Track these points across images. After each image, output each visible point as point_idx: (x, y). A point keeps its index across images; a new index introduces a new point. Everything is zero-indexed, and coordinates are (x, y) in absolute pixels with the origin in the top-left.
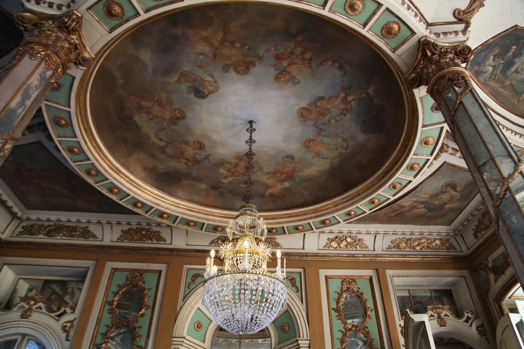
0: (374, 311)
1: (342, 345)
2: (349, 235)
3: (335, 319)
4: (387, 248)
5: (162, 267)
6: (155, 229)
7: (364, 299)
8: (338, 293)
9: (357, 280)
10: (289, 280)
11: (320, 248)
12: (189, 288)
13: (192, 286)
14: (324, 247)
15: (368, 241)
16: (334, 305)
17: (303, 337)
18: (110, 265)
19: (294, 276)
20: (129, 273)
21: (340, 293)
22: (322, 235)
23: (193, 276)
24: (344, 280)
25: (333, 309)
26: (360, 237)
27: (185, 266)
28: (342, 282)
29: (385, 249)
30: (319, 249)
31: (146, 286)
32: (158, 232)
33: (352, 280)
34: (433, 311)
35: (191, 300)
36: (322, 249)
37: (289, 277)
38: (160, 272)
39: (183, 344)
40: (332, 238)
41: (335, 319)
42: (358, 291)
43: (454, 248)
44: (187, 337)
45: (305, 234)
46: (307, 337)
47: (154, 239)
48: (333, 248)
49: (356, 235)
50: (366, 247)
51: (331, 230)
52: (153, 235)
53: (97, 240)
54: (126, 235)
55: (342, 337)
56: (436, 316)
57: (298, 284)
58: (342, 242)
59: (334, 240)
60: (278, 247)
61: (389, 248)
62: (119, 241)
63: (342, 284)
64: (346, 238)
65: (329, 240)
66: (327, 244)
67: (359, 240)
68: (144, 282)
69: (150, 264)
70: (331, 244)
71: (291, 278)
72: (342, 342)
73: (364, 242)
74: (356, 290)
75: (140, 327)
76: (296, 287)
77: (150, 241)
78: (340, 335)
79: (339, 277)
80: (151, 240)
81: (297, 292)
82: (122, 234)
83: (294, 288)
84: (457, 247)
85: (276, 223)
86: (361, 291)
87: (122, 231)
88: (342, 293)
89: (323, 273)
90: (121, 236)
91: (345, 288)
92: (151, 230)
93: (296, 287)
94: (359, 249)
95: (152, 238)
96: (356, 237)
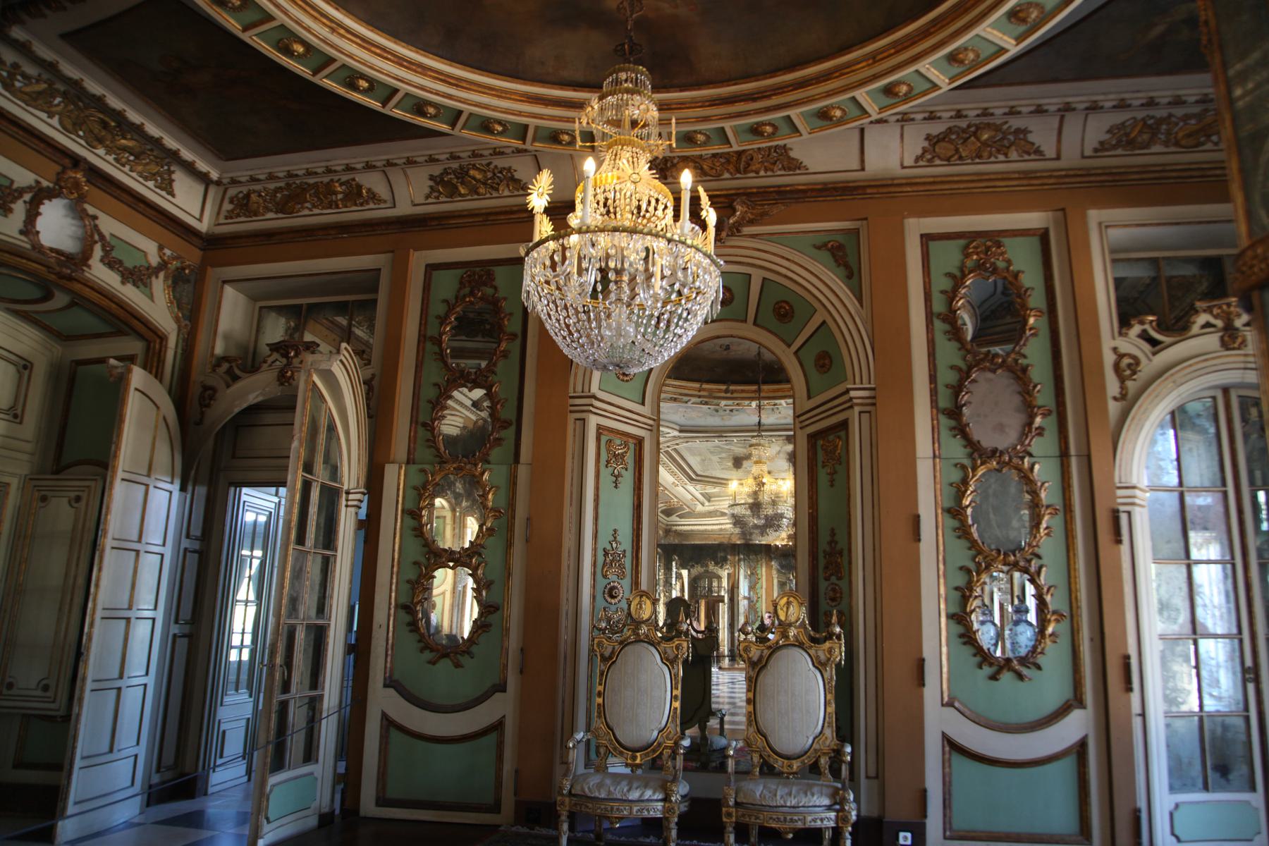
2: (986, 120)
3: (940, 339)
6: (500, 162)
7: (1022, 287)
9: (1006, 241)
10: (829, 250)
11: (906, 164)
14: (917, 160)
15: (1042, 134)
16: (939, 306)
17: (862, 383)
18: (419, 260)
20: (464, 270)
21: (958, 274)
22: (909, 129)
24: (970, 237)
25: (939, 315)
26: (1015, 123)
28: (967, 247)
29: (1088, 152)
30: (903, 167)
32: (509, 169)
33: (995, 238)
34: (1211, 313)
36: (913, 164)
37: (829, 242)
39: (591, 408)
40: (936, 134)
41: (940, 339)
42: (1007, 269)
44: (600, 395)
45: (862, 131)
46: (870, 383)
47: (501, 188)
48: (942, 159)
49: (1006, 118)
50: (1038, 151)
51: (931, 112)
52: (498, 177)
53: (382, 206)
54: (444, 184)
56: (1219, 323)
58: (966, 140)
59: (944, 138)
60: (798, 172)
61: (1102, 147)
62: (430, 200)
63: (967, 256)
64: (975, 134)
65: (930, 140)
66: (925, 151)
67: (1018, 131)
68: (496, 288)
70: (934, 150)
71: (832, 245)
72: (957, 390)
73: (1031, 138)
74: (1001, 264)
76: (847, 266)
77: (495, 194)
80: (497, 190)
81: (850, 276)
82: (431, 183)
83: (842, 268)
85: (768, 110)
87: (432, 178)
88: (964, 276)
89: (916, 227)
90: (431, 187)
91: (969, 263)
92: (492, 166)
95: (498, 184)
96: (1005, 127)
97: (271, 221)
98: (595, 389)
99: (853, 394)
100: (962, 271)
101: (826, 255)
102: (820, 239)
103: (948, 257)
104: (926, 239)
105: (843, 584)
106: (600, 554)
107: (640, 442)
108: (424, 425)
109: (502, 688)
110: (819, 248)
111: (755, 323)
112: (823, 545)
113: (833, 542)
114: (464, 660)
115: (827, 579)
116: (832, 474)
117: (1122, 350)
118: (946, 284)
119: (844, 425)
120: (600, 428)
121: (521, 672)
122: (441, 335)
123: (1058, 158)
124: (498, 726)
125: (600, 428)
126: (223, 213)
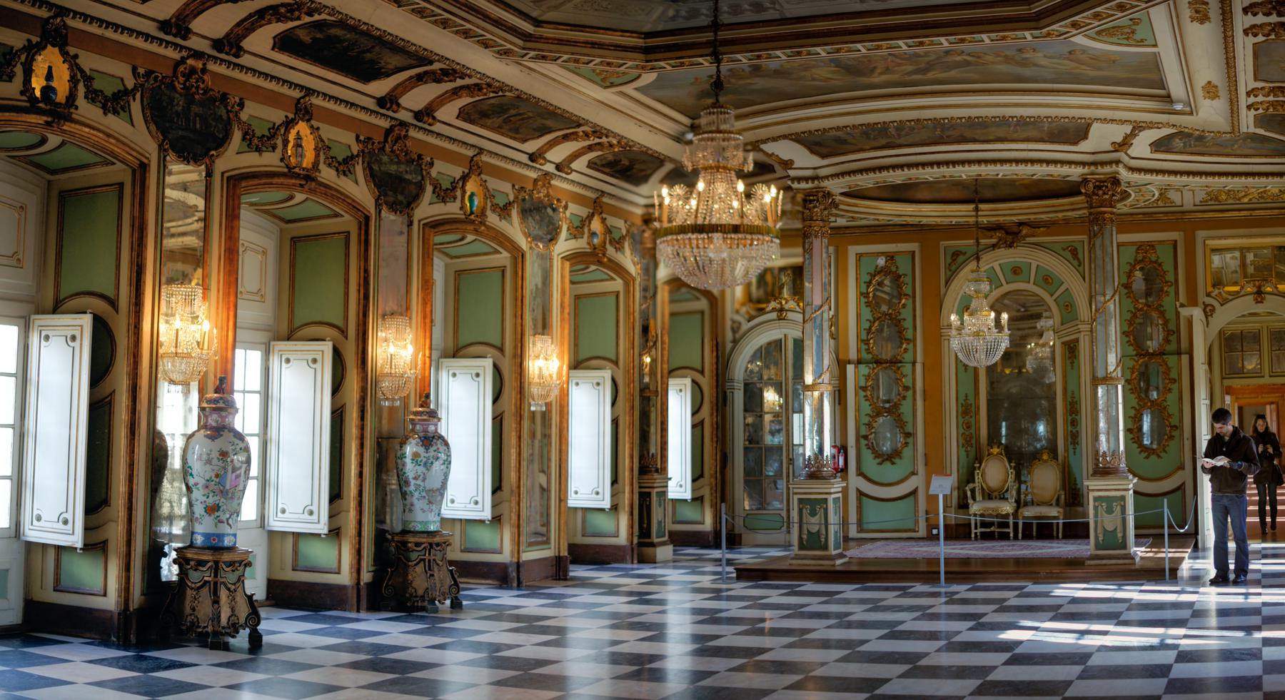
0: (1173, 287)
1: (1129, 328)
4: (1201, 202)
5: (914, 246)
8: (1131, 264)
9: (1157, 247)
12: (950, 270)
13: (953, 268)
16: (1124, 280)
18: (853, 250)
19: (1076, 245)
23: (953, 254)
24: (1140, 246)
27: (941, 243)
28: (1138, 249)
29: (1198, 203)
31: (900, 272)
33: (1152, 245)
35: (954, 285)
55: (1131, 318)
57: (1080, 256)
63: (1137, 253)
68: (897, 267)
69: (899, 245)
74: (1153, 259)
75: (904, 319)
79: (1132, 243)
81: (1079, 266)
86: (1160, 261)
91: (1140, 258)
93: (1078, 259)
94: (1162, 205)
99: (1080, 326)
100: (1135, 260)
101: (1069, 255)
103: (1129, 254)
105: (1078, 418)
106: (960, 405)
108: (862, 341)
109: (913, 473)
110: (1064, 250)
111: (1034, 284)
114: (897, 461)
115: (1071, 415)
117: (1207, 303)
118: (1128, 268)
119: (1077, 340)
121: (926, 465)
122: (868, 293)
123: (1182, 206)
124: (914, 493)
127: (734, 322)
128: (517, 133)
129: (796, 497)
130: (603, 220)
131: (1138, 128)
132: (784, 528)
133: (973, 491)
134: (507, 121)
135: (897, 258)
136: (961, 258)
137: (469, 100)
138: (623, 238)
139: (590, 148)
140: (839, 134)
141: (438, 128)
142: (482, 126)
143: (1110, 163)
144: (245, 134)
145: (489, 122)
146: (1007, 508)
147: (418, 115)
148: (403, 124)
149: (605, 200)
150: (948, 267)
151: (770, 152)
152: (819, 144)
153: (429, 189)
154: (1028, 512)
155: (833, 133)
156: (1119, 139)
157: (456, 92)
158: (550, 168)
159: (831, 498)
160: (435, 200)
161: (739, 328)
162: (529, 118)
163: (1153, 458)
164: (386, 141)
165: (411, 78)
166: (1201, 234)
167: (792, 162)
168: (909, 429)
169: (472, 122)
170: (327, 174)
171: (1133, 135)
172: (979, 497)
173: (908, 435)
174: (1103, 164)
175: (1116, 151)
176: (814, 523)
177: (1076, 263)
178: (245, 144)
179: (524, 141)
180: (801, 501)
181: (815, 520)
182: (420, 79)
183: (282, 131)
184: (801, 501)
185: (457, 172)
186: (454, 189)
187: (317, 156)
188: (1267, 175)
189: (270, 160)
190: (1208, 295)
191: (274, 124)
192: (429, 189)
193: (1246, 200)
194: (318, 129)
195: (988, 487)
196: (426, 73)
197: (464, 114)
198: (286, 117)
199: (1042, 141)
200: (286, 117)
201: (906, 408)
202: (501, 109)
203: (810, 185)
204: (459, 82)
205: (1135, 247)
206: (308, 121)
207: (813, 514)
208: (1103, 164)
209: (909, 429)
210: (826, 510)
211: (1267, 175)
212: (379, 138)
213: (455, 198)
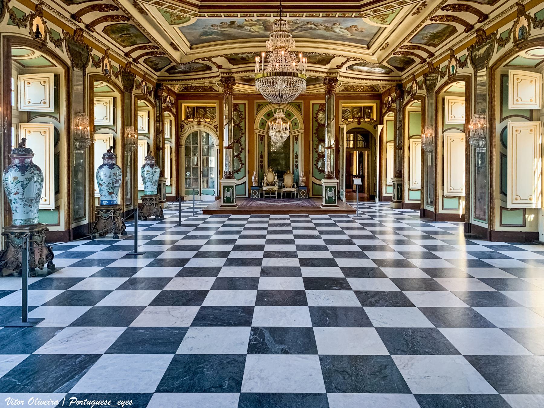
3: (314, 122)
5: (246, 102)
13: (259, 109)
16: (315, 116)
24: (321, 104)
31: (241, 110)
38: (245, 104)
41: (314, 122)
43: (375, 90)
57: (301, 107)
61: (343, 90)
63: (320, 107)
72: (317, 130)
78: (316, 128)
84: (377, 89)
89: (312, 102)
97: (192, 92)
98: (258, 129)
101: (297, 107)
102: (296, 104)
103: (317, 107)
104: (313, 104)
107: (264, 136)
109: (244, 177)
112: (295, 154)
113: (296, 153)
116: (296, 142)
118: (316, 112)
120: (259, 135)
124: (245, 183)
125: (259, 135)
126: (181, 90)
127: (181, 125)
128: (123, 43)
129: (222, 185)
130: (146, 83)
131: (348, 60)
132: (199, 194)
133: (263, 182)
134: (120, 37)
135: (239, 105)
136: (261, 107)
137: (111, 23)
138: (151, 91)
139: (147, 54)
140: (243, 56)
141: (94, 34)
142: (111, 37)
143: (335, 73)
144: (11, 15)
145: (113, 36)
146: (275, 188)
147: (87, 26)
148: (81, 29)
149: (147, 76)
150: (257, 109)
151: (214, 62)
152: (234, 59)
153: (91, 61)
154: (285, 190)
155: (241, 55)
156: (339, 64)
157: (105, 19)
158: (131, 60)
159: (234, 185)
160: (93, 66)
161: (184, 127)
162: (131, 36)
163: (322, 173)
164: (74, 35)
165: (89, 6)
166: (341, 101)
167: (221, 66)
168: (243, 162)
169: (108, 35)
170: (50, 45)
171: (345, 62)
172: (265, 185)
173: (243, 164)
174: (332, 73)
175: (338, 68)
176: (228, 194)
177: (299, 109)
178: (11, 21)
179: (125, 47)
180: (224, 186)
181: (229, 193)
182: (93, 8)
183: (29, 18)
184: (224, 186)
185: (100, 55)
186: (100, 62)
187: (46, 35)
188: (380, 80)
189: (24, 32)
190: (342, 121)
191: (26, 14)
192: (91, 61)
193: (357, 90)
194: (46, 22)
195: (268, 182)
196: (97, 5)
197: (105, 30)
198: (31, 12)
199: (315, 63)
200: (31, 12)
201: (242, 155)
202: (122, 29)
203: (227, 75)
204: (111, 13)
205: (319, 105)
206: (41, 17)
207: (228, 191)
208: (332, 73)
209: (243, 162)
210: (233, 190)
211: (380, 80)
212: (72, 33)
213: (100, 66)
